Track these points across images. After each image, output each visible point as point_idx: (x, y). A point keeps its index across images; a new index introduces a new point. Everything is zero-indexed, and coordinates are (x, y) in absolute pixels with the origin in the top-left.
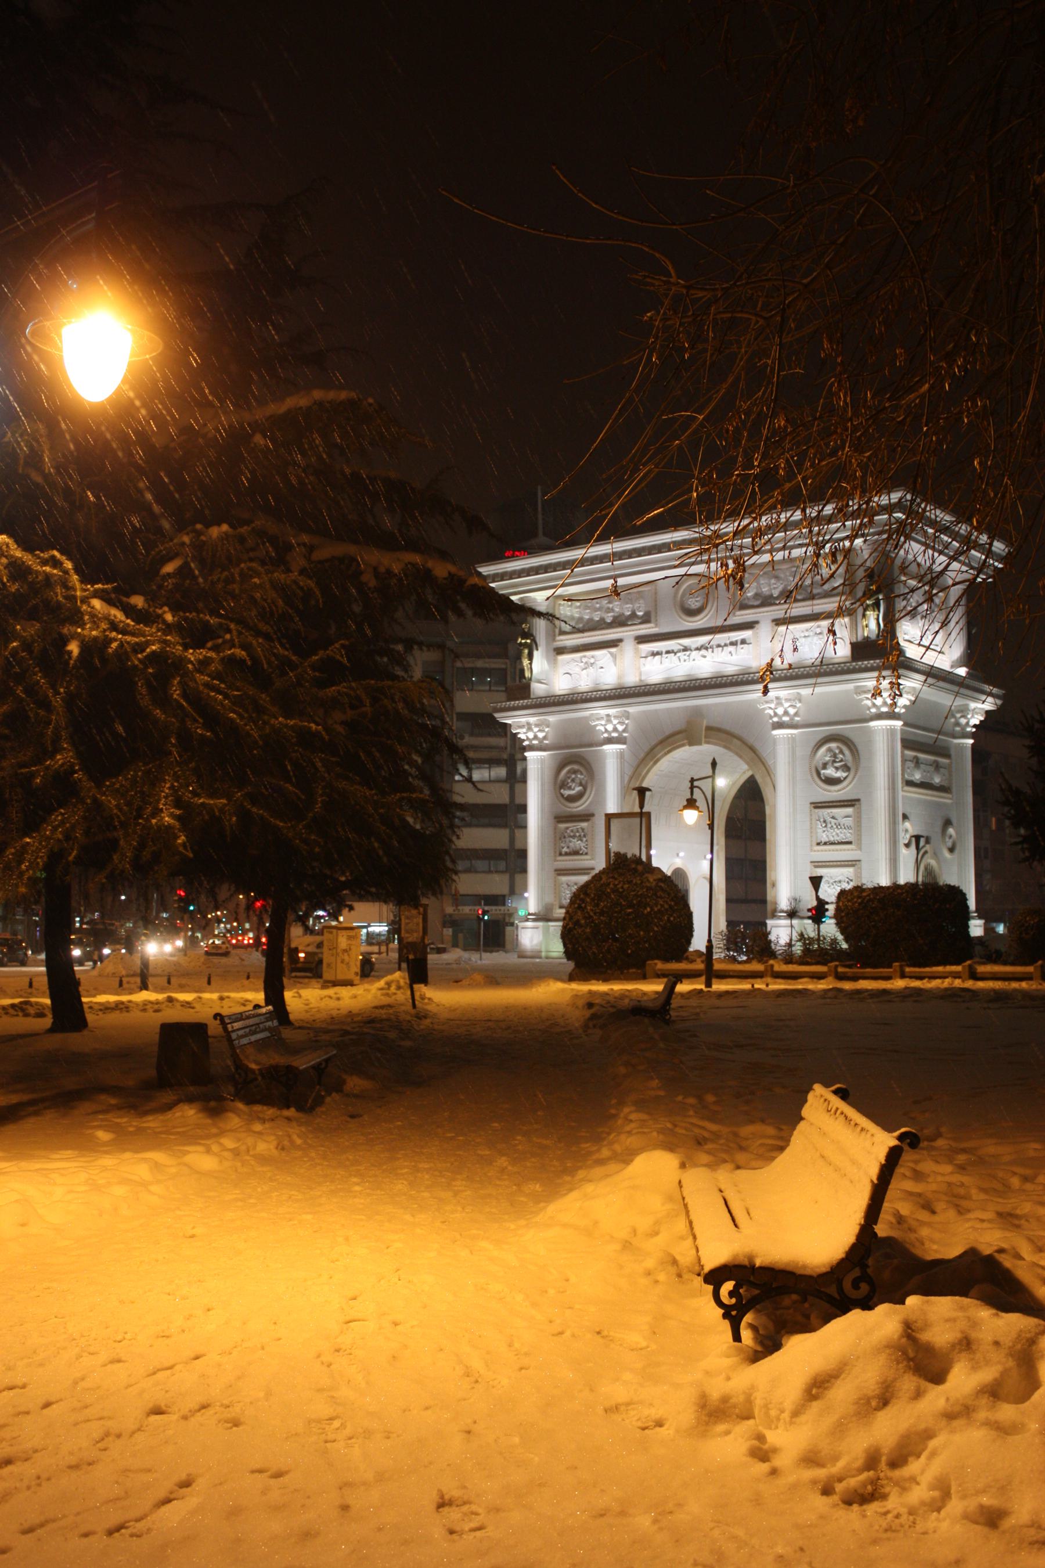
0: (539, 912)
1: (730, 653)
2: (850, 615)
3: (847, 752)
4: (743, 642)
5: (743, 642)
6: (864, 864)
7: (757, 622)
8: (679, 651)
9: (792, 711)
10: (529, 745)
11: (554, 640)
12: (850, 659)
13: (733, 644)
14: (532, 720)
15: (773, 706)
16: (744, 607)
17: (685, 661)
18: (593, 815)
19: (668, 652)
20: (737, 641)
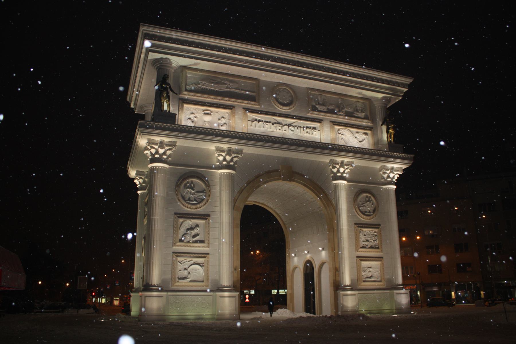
0: (160, 284)
1: (307, 132)
2: (370, 130)
3: (372, 198)
4: (314, 128)
5: (314, 128)
6: (384, 259)
7: (322, 120)
8: (275, 123)
9: (347, 171)
10: (158, 158)
11: (180, 92)
12: (388, 151)
13: (307, 128)
14: (167, 140)
15: (338, 166)
16: (314, 109)
17: (280, 130)
18: (209, 215)
19: (265, 122)
20: (310, 127)
